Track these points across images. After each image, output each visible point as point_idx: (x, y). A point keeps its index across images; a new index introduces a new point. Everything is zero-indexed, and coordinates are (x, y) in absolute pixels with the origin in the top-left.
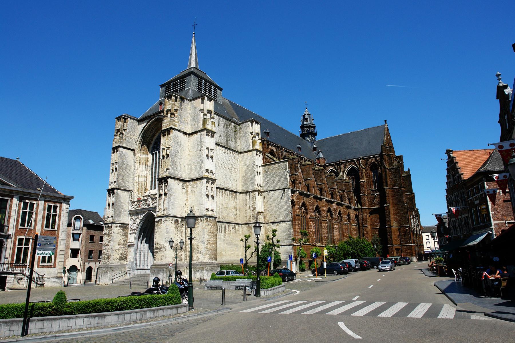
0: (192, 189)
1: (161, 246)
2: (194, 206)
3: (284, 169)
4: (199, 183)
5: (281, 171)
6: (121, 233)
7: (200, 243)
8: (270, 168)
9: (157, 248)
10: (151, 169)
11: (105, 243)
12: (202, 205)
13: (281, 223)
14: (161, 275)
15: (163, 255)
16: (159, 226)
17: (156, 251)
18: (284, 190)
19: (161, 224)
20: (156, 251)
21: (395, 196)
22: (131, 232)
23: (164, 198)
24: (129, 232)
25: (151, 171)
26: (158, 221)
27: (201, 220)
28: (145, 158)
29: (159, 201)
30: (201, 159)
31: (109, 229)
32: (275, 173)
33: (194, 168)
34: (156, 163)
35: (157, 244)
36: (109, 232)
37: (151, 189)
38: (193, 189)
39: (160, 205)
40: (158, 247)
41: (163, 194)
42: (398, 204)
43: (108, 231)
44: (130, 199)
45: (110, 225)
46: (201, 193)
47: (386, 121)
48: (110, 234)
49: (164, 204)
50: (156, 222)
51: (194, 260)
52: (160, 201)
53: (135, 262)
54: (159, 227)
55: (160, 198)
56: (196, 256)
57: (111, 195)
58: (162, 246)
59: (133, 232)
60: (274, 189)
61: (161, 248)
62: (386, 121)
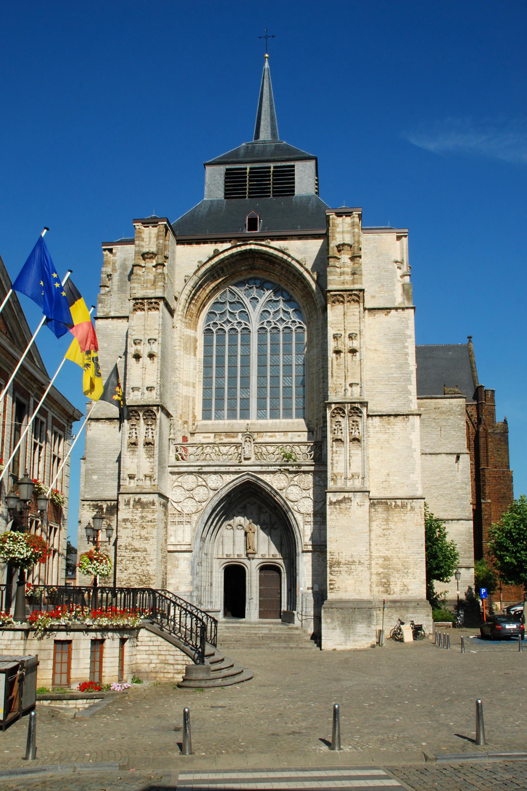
0: (379, 435)
1: (351, 560)
2: (388, 475)
3: (459, 415)
4: (400, 424)
5: (451, 417)
6: (163, 522)
7: (411, 557)
8: (423, 407)
9: (339, 563)
10: (202, 368)
11: (130, 545)
12: (411, 475)
13: (449, 523)
14: (362, 625)
15: (358, 579)
16: (341, 512)
17: (336, 569)
18: (458, 458)
19: (349, 509)
20: (336, 569)
21: (495, 486)
22: (177, 519)
23: (350, 450)
24: (170, 519)
25: (202, 373)
26: (339, 502)
27: (412, 507)
28: (192, 340)
29: (333, 453)
30: (403, 372)
31: (143, 508)
32: (434, 419)
33: (384, 390)
34: (220, 357)
35: (336, 554)
36: (142, 517)
37: (206, 416)
38: (385, 437)
39: (335, 465)
40: (343, 561)
41: (347, 439)
42: (500, 502)
43: (140, 515)
44: (172, 436)
45: (145, 498)
46: (409, 447)
47: (470, 338)
48: (151, 522)
49: (350, 463)
50: (331, 503)
51: (394, 593)
52: (334, 455)
53: (195, 594)
54: (341, 515)
55: (335, 449)
56: (399, 583)
57: (142, 421)
58: (356, 559)
59: (185, 519)
60: (431, 452)
61: (348, 564)
62: (470, 338)
